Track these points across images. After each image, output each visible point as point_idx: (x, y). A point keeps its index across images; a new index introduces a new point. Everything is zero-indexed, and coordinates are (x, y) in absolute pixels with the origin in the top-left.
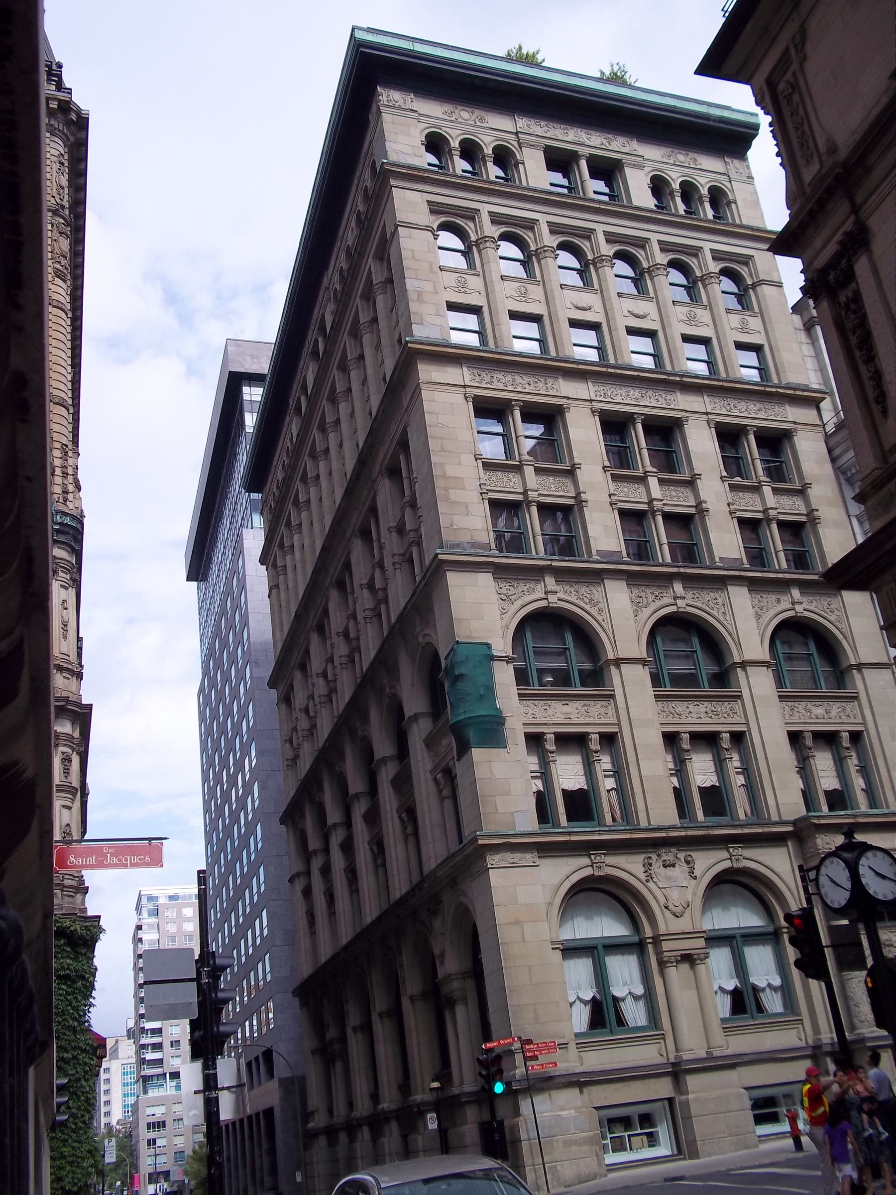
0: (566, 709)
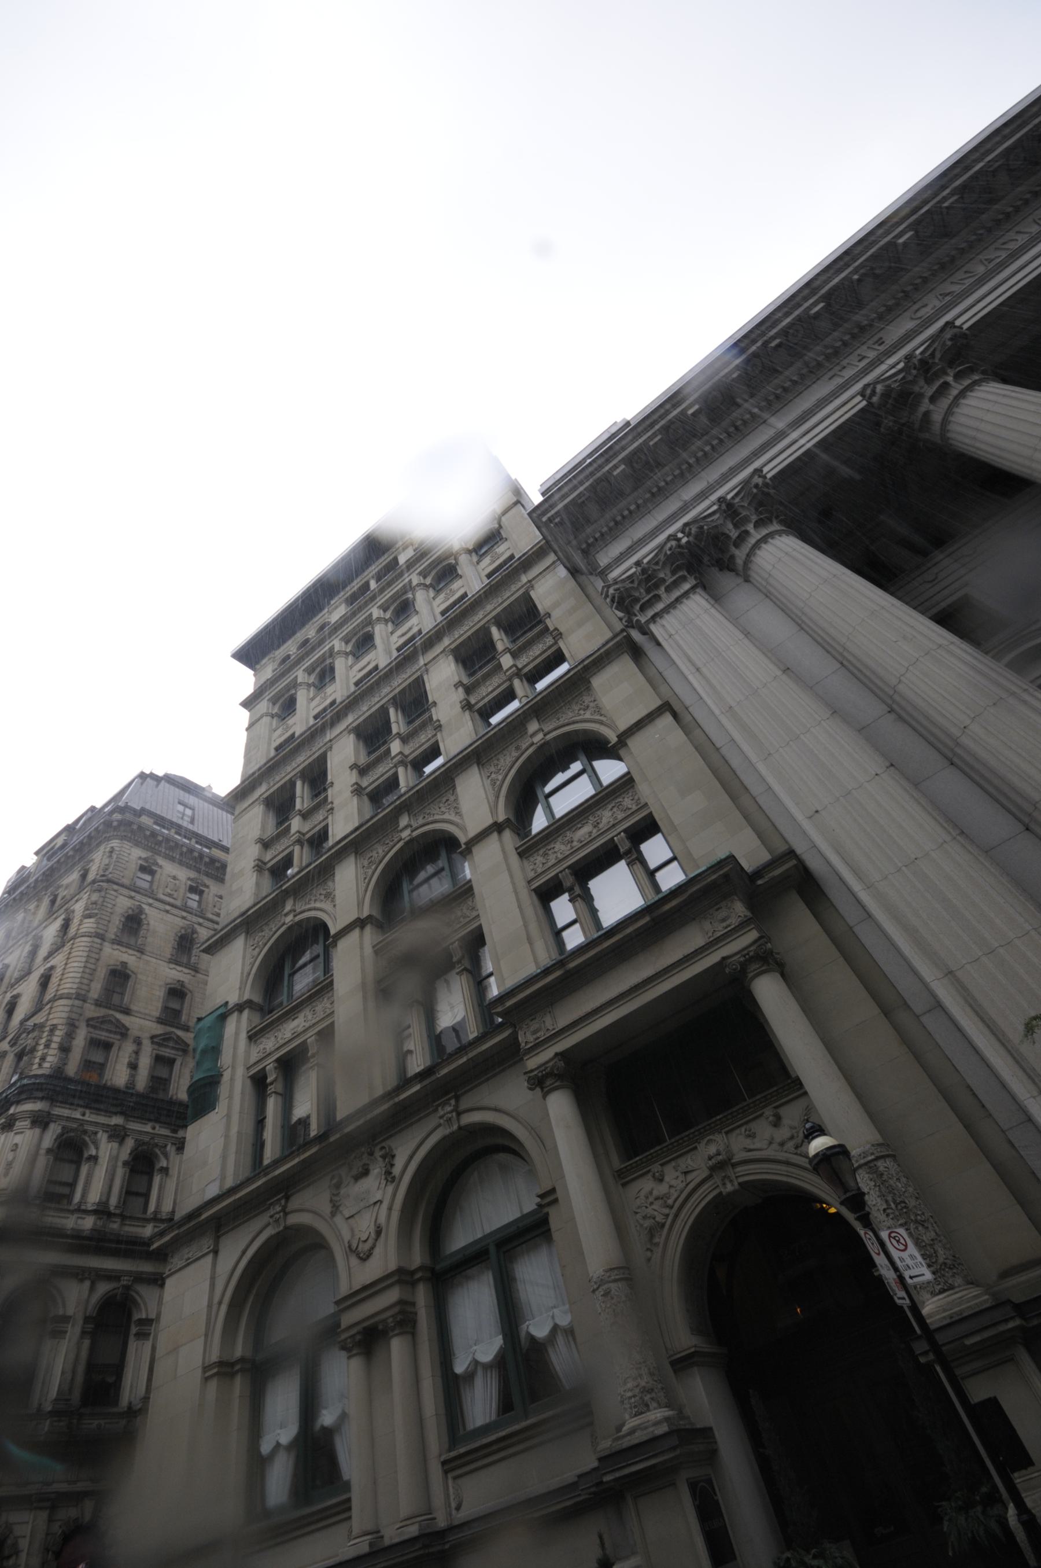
0: (296, 1022)
